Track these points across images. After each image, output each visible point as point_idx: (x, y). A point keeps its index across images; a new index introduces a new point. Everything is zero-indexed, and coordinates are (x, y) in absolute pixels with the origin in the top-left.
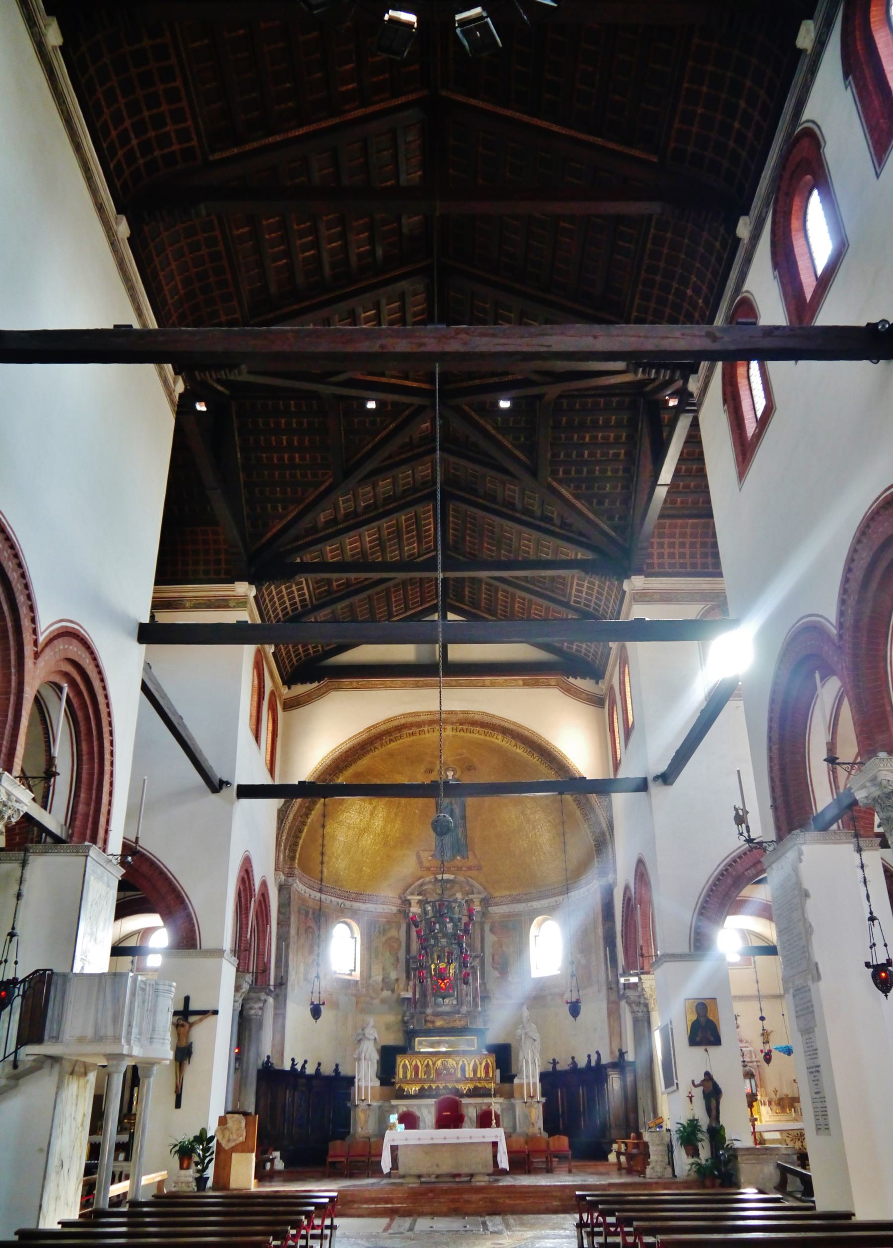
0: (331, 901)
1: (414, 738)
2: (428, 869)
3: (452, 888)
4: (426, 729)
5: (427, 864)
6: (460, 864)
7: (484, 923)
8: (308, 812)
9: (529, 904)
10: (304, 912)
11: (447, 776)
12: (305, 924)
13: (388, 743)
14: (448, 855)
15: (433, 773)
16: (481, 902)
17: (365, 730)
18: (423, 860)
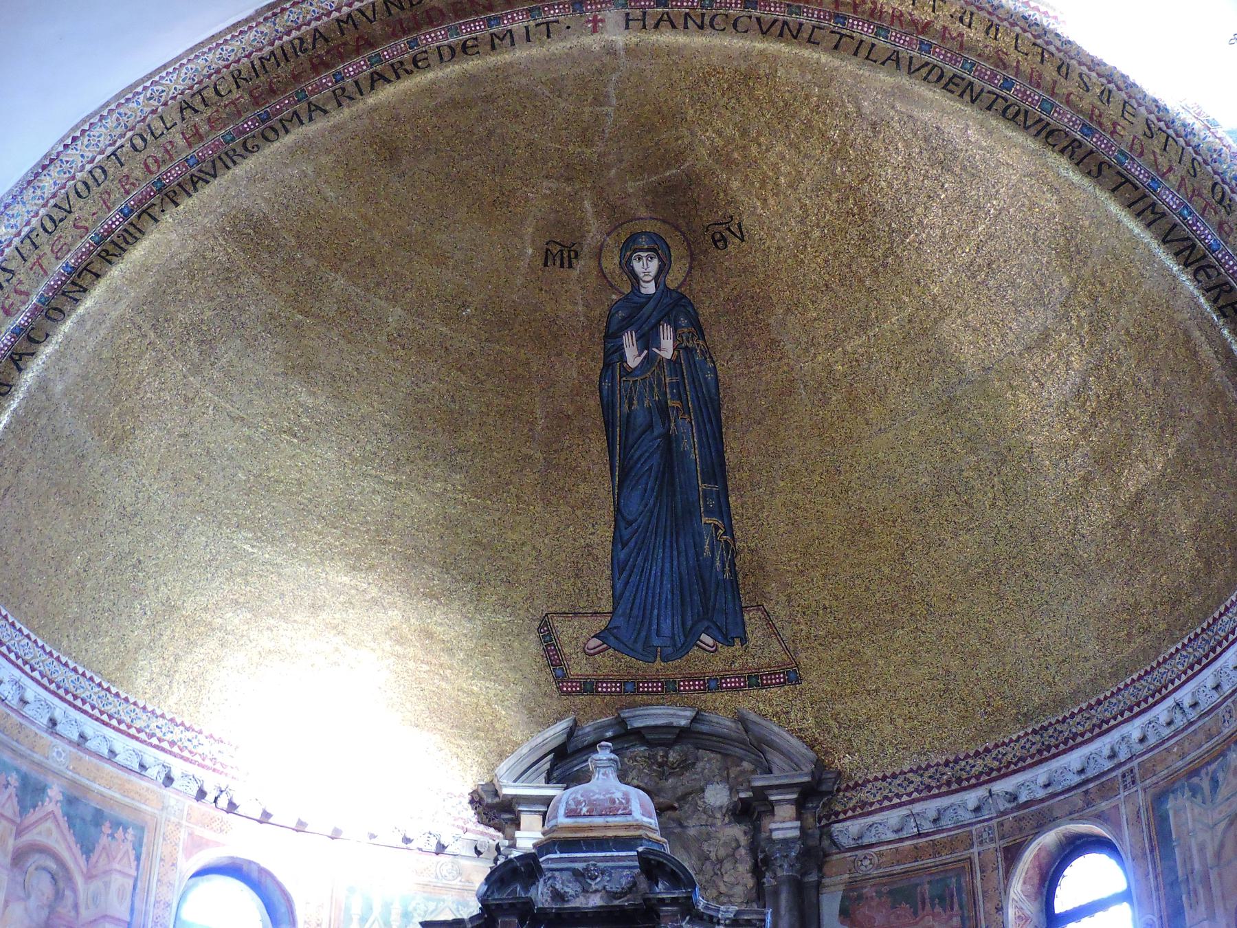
0: (169, 780)
1: (472, 65)
2: (588, 687)
3: (685, 765)
4: (518, 27)
5: (579, 668)
6: (717, 665)
7: (818, 886)
8: (24, 346)
9: (1000, 787)
10: (14, 779)
11: (635, 279)
12: (19, 834)
13: (365, 85)
14: (666, 627)
15: (580, 265)
16: (800, 805)
17: (259, 13)
18: (566, 650)
